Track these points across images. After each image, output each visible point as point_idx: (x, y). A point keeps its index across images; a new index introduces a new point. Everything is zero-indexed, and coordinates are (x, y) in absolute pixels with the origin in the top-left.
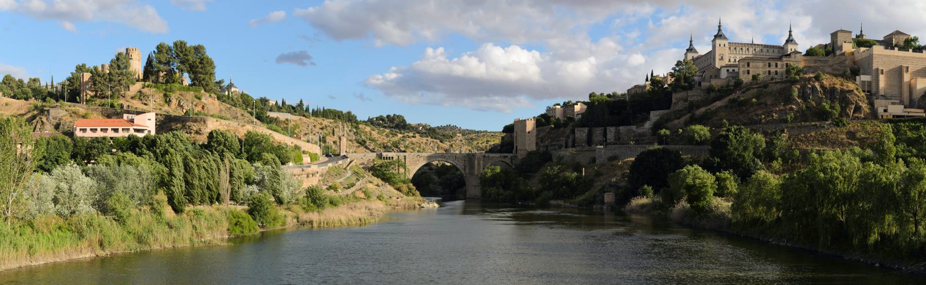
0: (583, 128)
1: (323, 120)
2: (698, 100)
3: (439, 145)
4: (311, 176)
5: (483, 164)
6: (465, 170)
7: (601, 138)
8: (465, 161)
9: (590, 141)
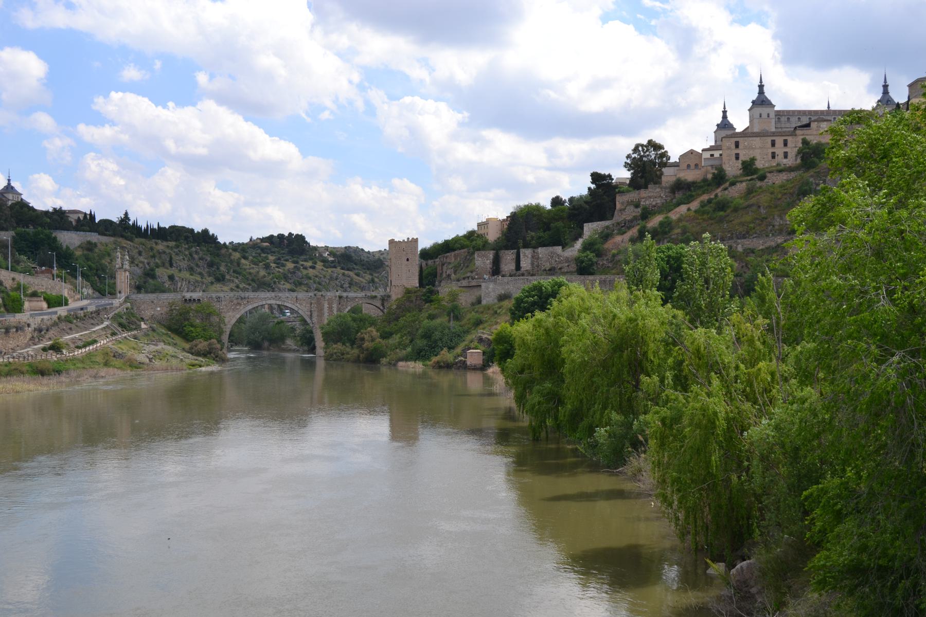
0: (487, 252)
1: (156, 244)
2: (657, 204)
3: (352, 280)
4: (15, 330)
6: (311, 318)
7: (512, 266)
8: (311, 304)
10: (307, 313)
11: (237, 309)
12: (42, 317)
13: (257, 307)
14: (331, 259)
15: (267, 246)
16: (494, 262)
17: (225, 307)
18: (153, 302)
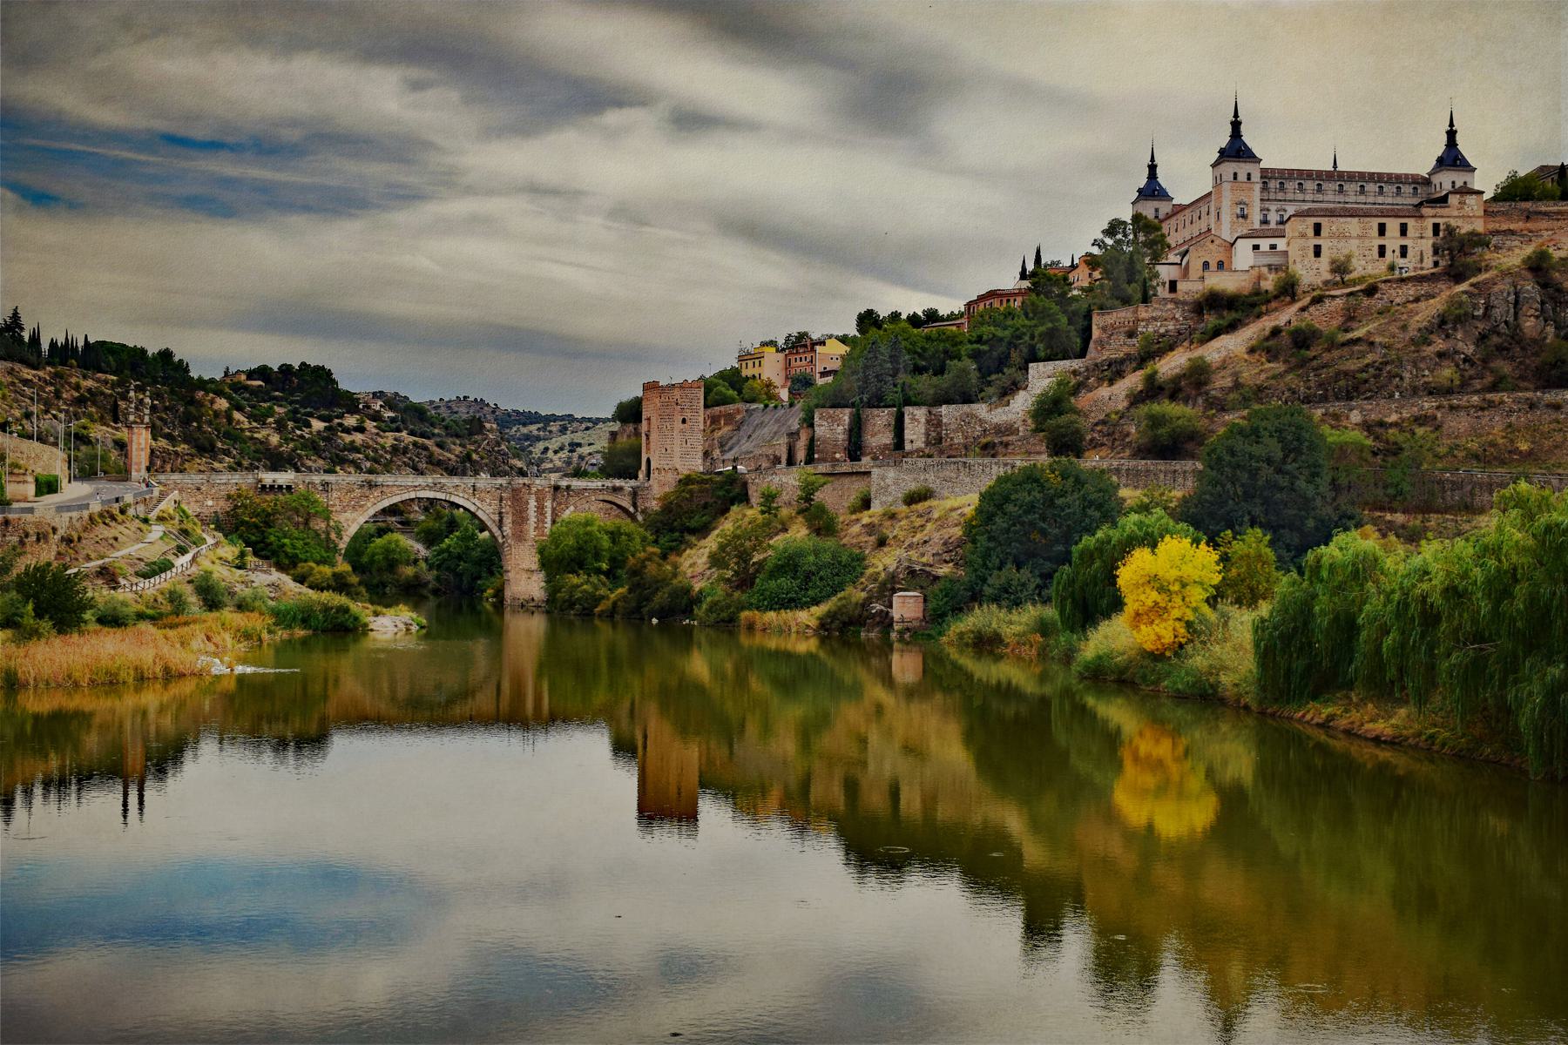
2: (1167, 331)
5: (554, 509)
7: (887, 438)
8: (501, 500)
9: (855, 449)
10: (492, 516)
11: (362, 506)
12: (69, 514)
13: (412, 500)
14: (388, 414)
15: (261, 386)
16: (851, 430)
17: (337, 502)
18: (199, 489)
